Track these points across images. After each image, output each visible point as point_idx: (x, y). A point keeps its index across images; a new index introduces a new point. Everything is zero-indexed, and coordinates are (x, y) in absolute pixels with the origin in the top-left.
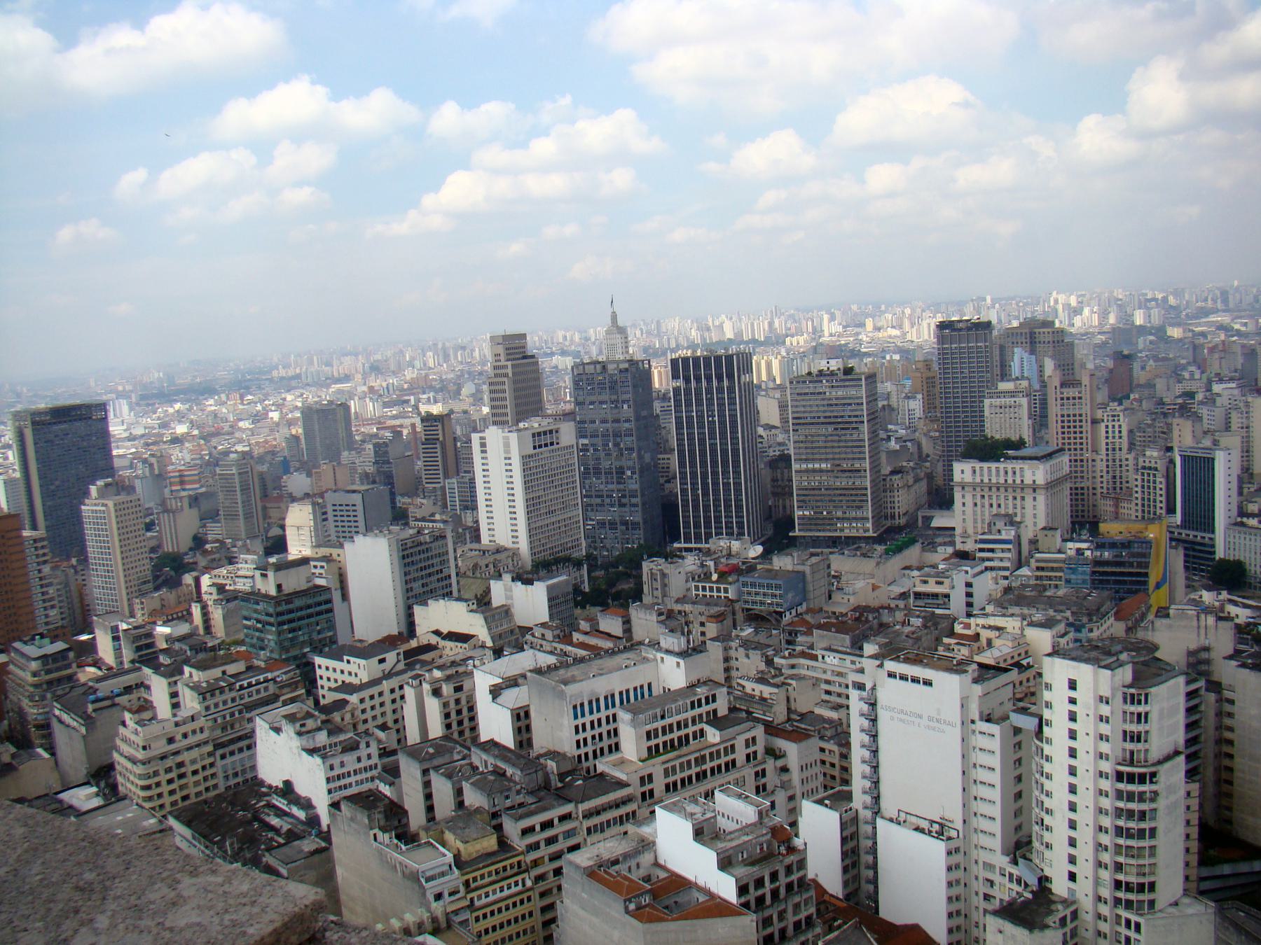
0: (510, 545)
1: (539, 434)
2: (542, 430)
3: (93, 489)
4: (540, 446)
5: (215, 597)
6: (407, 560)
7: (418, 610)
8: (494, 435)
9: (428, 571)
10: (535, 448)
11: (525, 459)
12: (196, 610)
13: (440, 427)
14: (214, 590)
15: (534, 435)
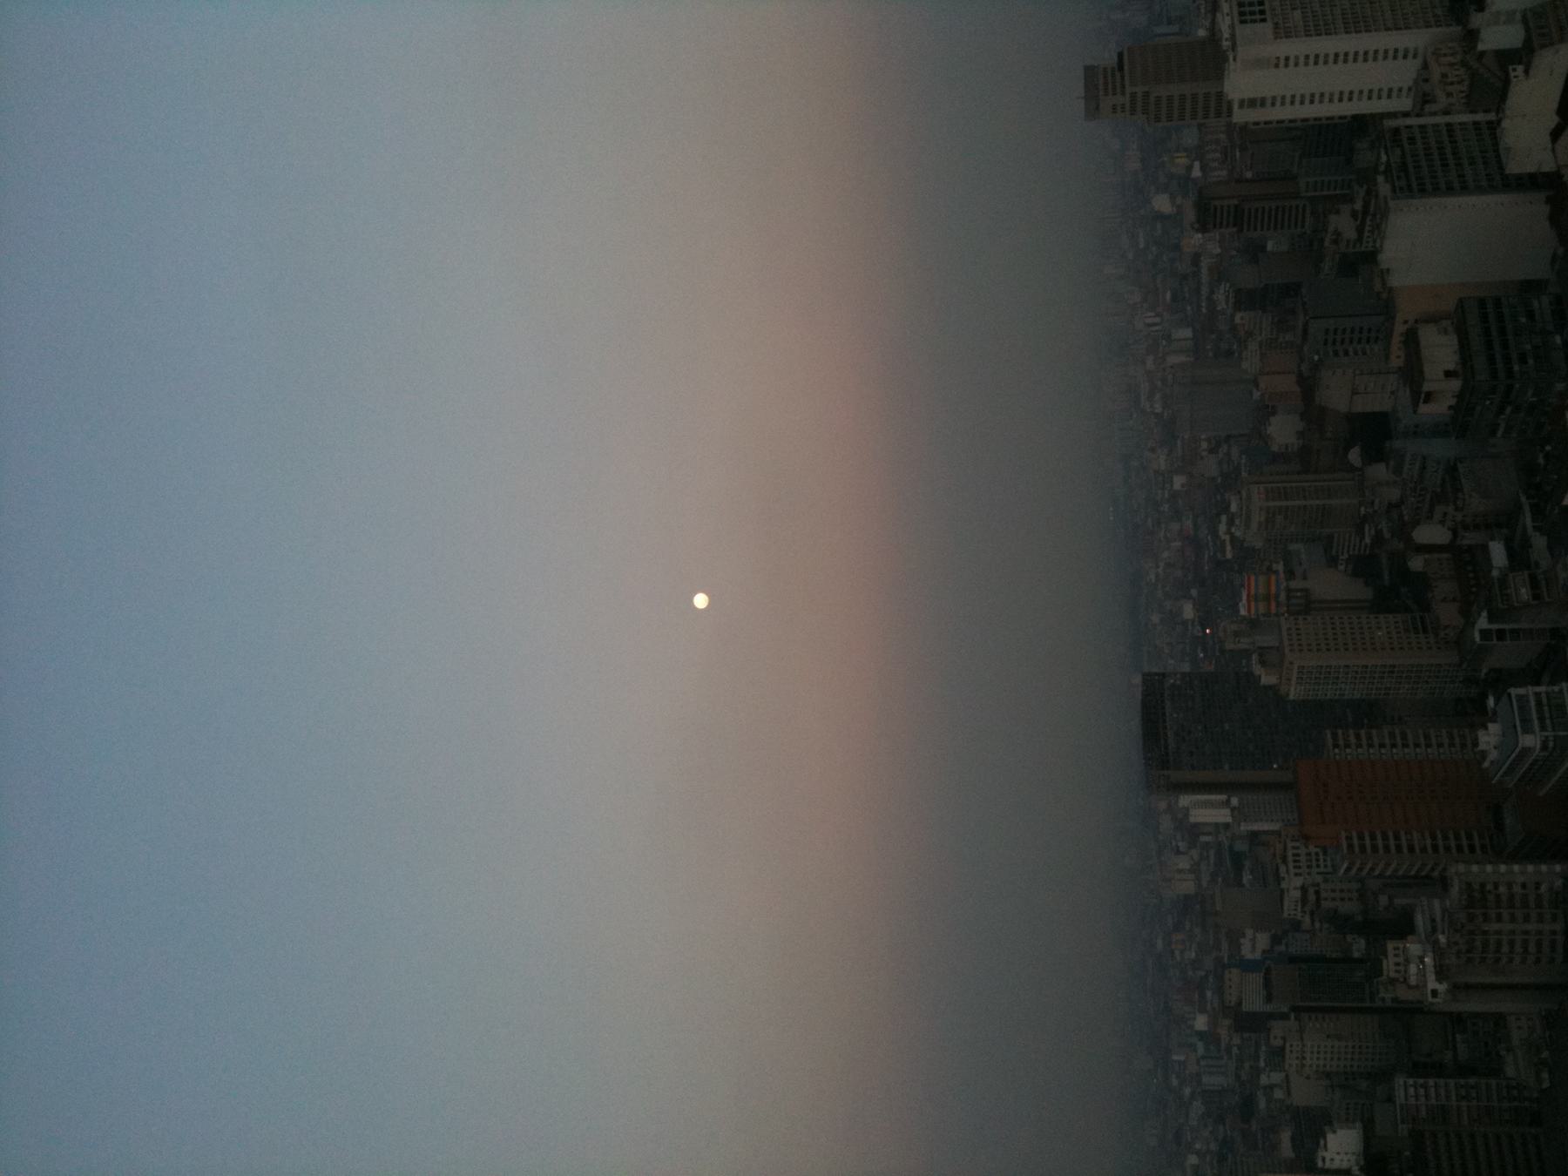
0: (1419, 61)
1: (1241, 14)
2: (1235, 10)
3: (1267, 679)
4: (1262, 12)
5: (1451, 509)
6: (1429, 187)
7: (1513, 168)
8: (1240, 83)
9: (1450, 156)
10: (1264, 20)
11: (1283, 32)
12: (1469, 539)
13: (1217, 203)
14: (1439, 510)
15: (1242, 22)
